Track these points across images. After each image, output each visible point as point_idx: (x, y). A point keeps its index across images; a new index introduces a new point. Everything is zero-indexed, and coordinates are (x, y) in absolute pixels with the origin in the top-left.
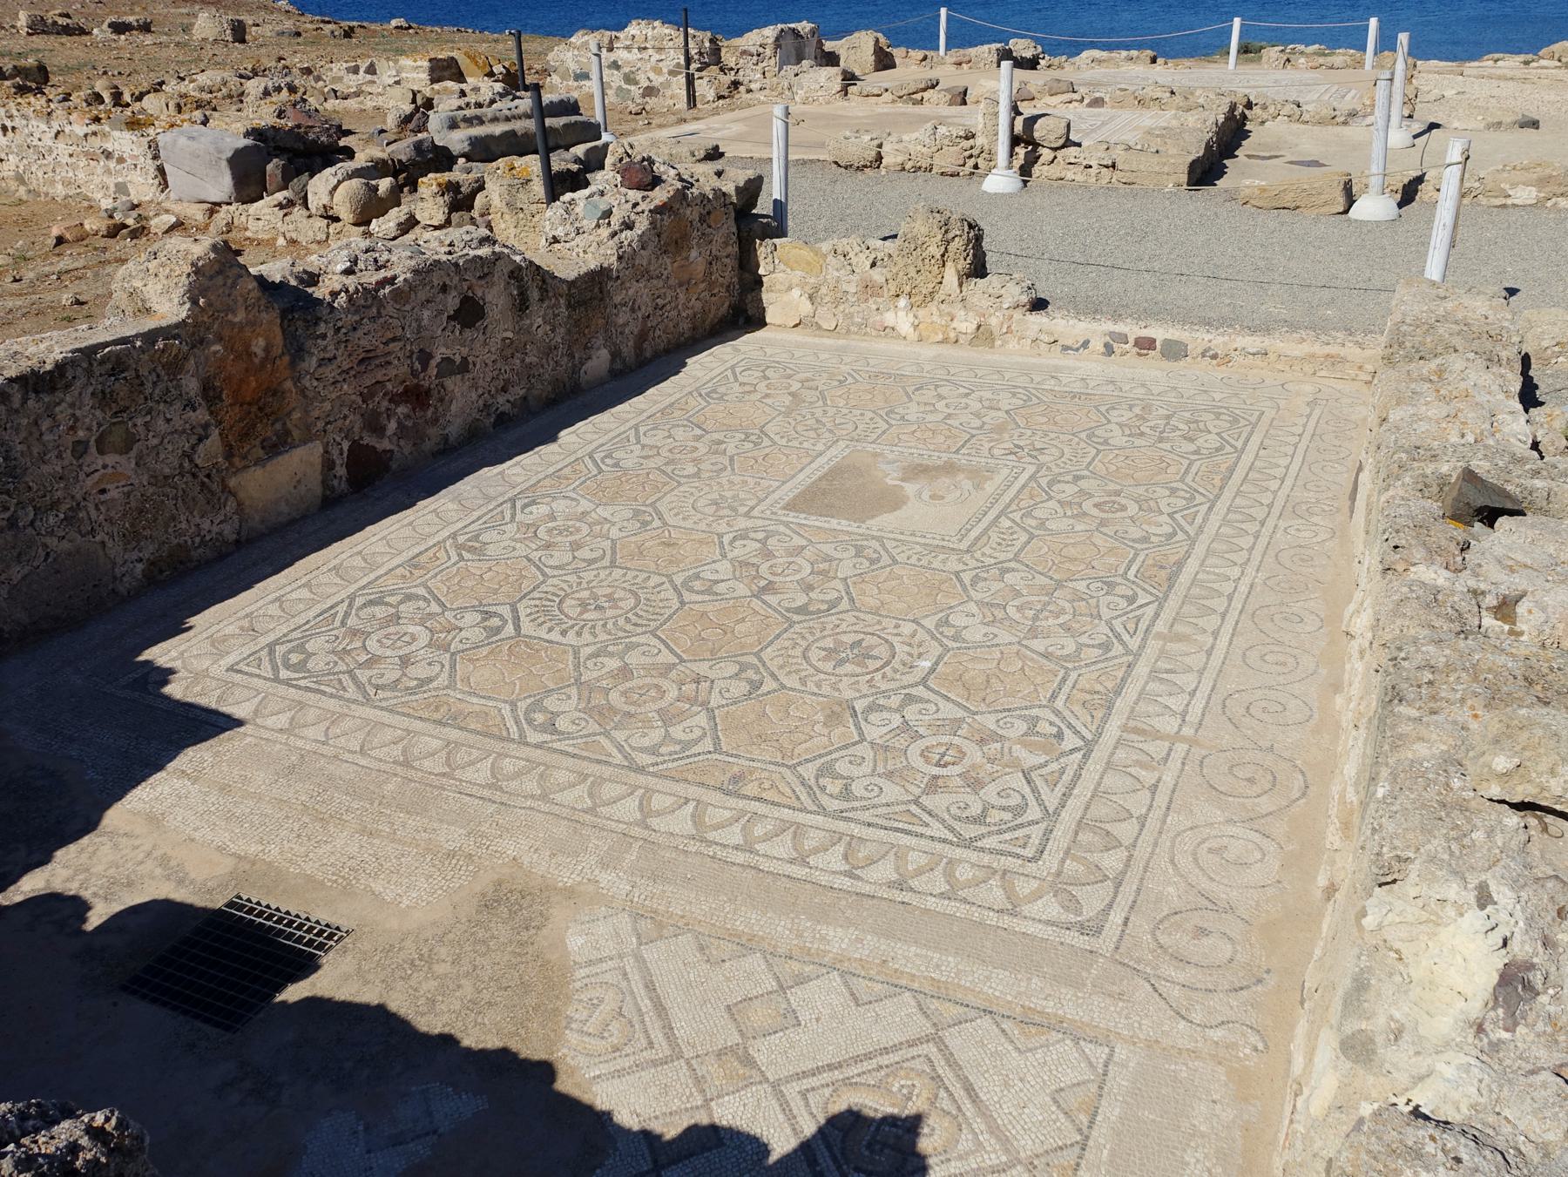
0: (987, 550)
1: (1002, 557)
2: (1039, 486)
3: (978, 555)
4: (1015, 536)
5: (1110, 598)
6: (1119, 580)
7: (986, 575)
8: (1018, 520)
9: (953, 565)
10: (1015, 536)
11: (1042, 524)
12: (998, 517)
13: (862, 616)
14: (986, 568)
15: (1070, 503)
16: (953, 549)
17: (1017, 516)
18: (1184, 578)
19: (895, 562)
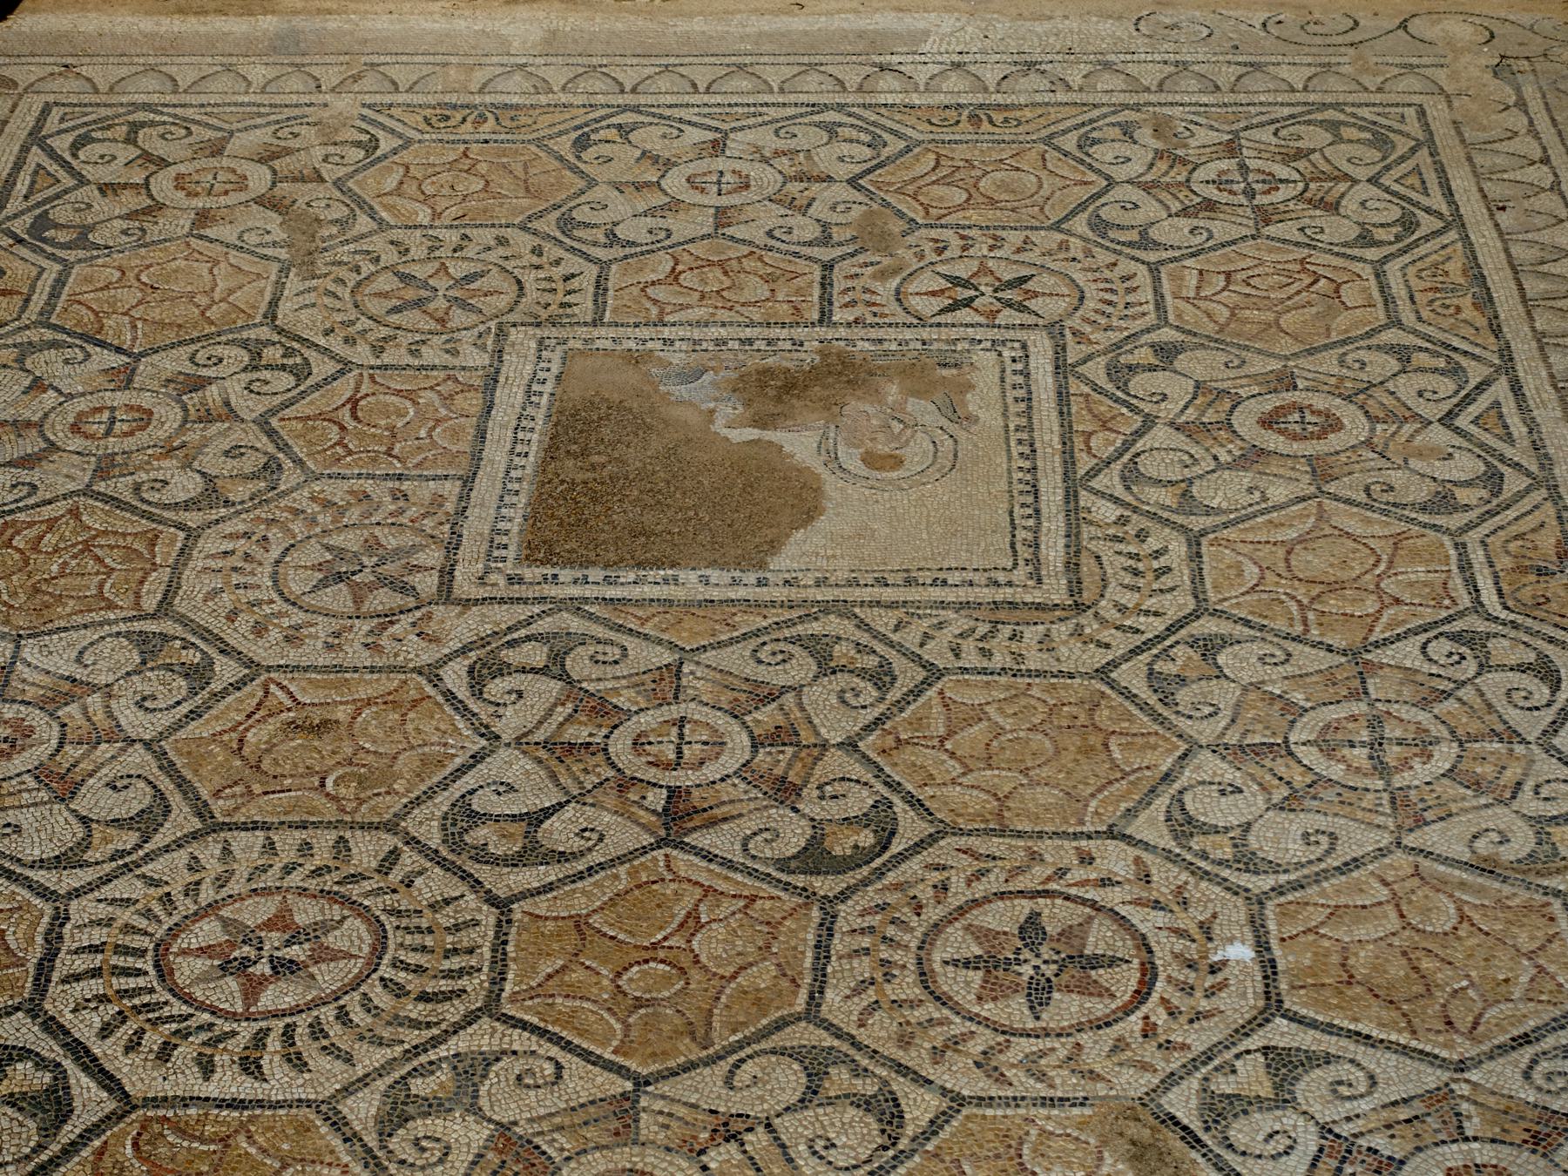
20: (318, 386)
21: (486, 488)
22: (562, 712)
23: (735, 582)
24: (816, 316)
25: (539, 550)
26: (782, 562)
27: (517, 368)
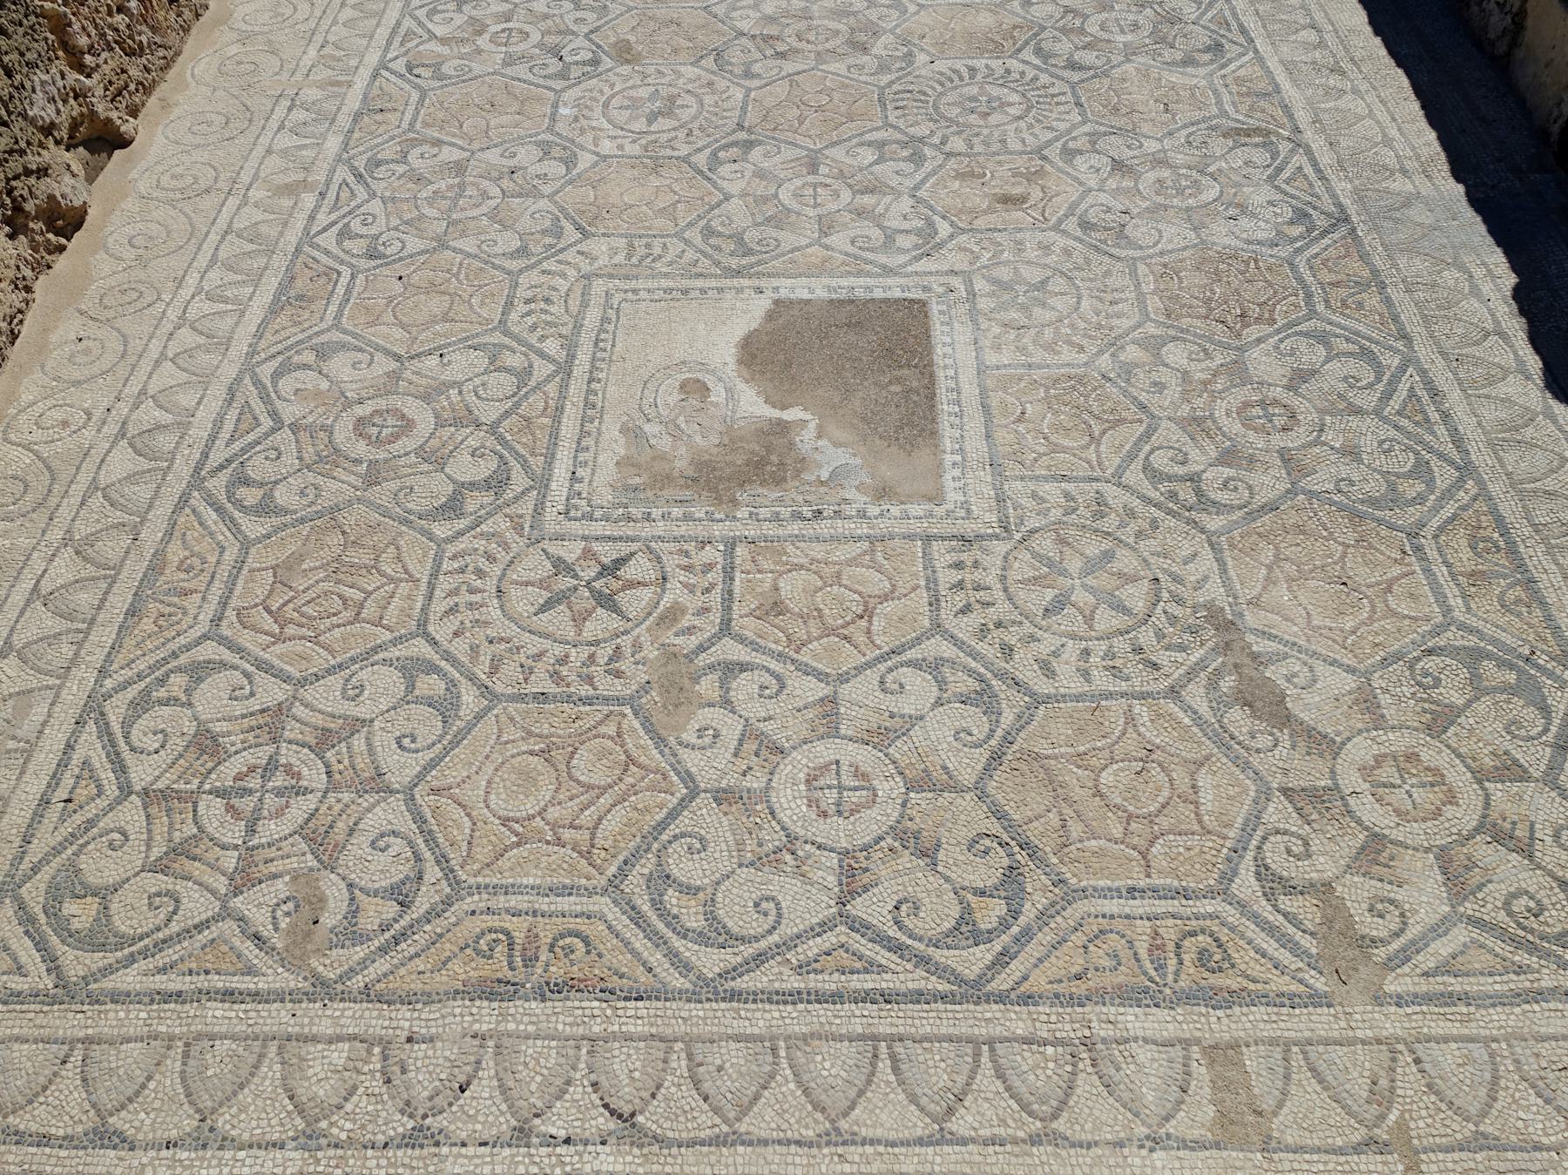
0: (563, 285)
1: (534, 277)
2: (525, 465)
4: (530, 320)
5: (373, 231)
6: (364, 264)
7: (548, 240)
8: (537, 362)
9: (599, 247)
10: (530, 320)
12: (571, 357)
13: (669, 152)
15: (458, 423)
16: (611, 276)
18: (271, 283)
23: (792, 290)
24: (739, 551)
26: (763, 304)
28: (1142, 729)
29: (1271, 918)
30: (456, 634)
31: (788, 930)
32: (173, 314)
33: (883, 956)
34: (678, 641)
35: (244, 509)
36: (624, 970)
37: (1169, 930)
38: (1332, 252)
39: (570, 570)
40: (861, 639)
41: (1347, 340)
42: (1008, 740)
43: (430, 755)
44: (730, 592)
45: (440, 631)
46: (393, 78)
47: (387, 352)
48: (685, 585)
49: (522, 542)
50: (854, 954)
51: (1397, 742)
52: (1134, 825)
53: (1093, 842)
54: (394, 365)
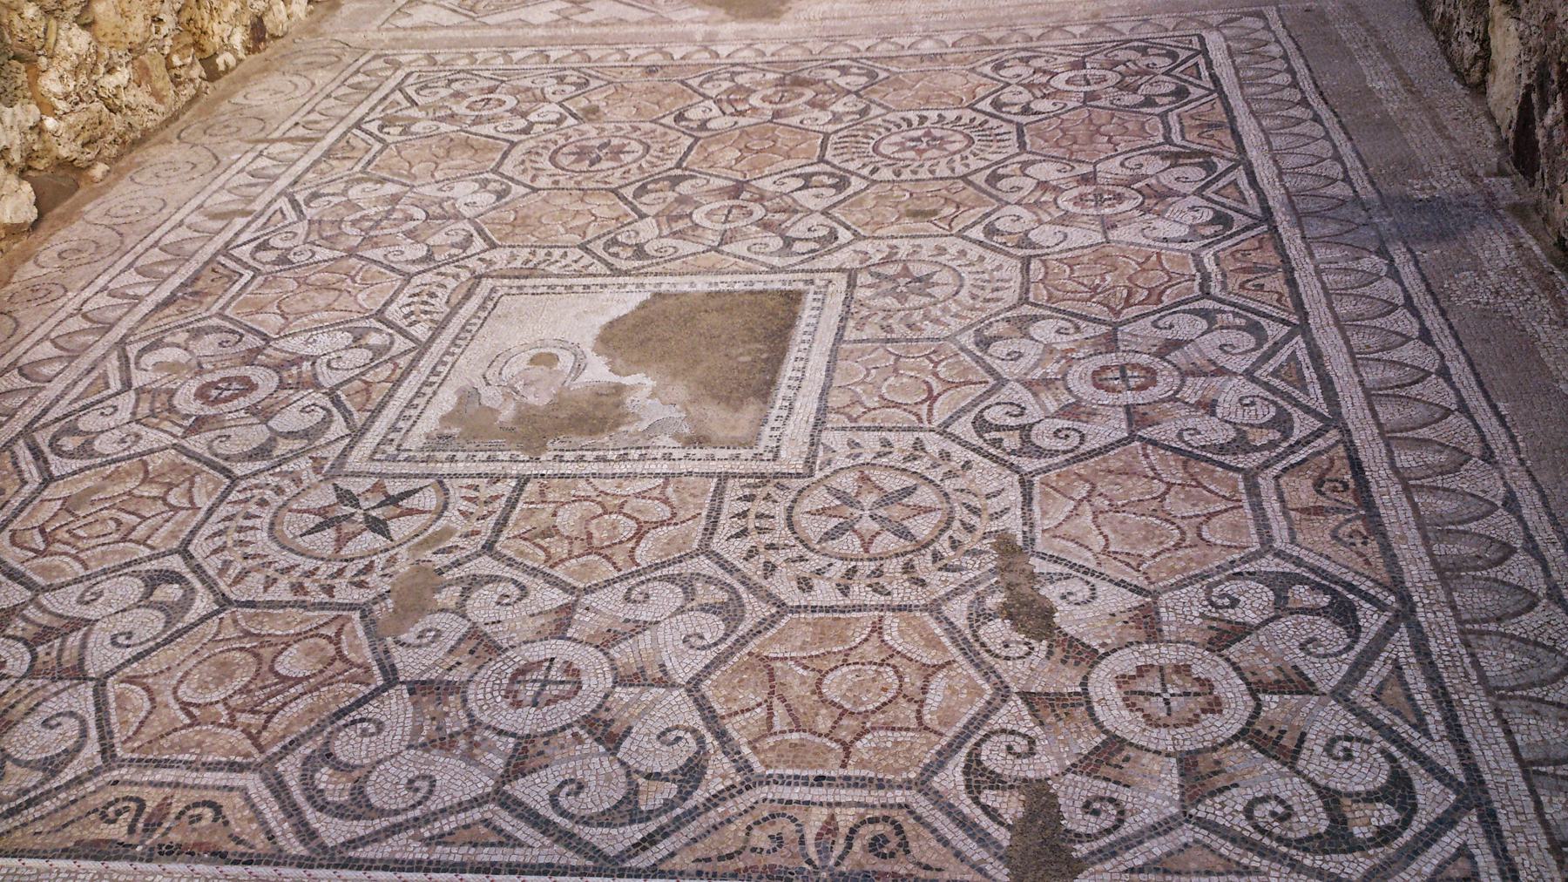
3: (465, 275)
7: (454, 251)
8: (399, 339)
9: (500, 257)
10: (406, 310)
11: (358, 339)
12: (432, 339)
13: (601, 185)
14: (452, 260)
16: (503, 277)
17: (401, 344)
19: (583, 247)
20: (964, 410)
21: (826, 338)
22: (788, 224)
23: (674, 285)
25: (792, 299)
27: (798, 428)
28: (886, 638)
29: (966, 811)
30: (215, 552)
31: (434, 805)
32: (70, 308)
33: (523, 831)
34: (435, 558)
35: (60, 453)
36: (244, 837)
37: (846, 819)
38: (1244, 245)
39: (353, 500)
40: (620, 559)
41: (1236, 315)
42: (742, 642)
43: (140, 649)
44: (506, 520)
45: (199, 549)
46: (363, 135)
47: (258, 333)
48: (462, 513)
49: (315, 479)
50: (494, 828)
51: (1168, 655)
52: (844, 722)
53: (795, 736)
54: (259, 342)
